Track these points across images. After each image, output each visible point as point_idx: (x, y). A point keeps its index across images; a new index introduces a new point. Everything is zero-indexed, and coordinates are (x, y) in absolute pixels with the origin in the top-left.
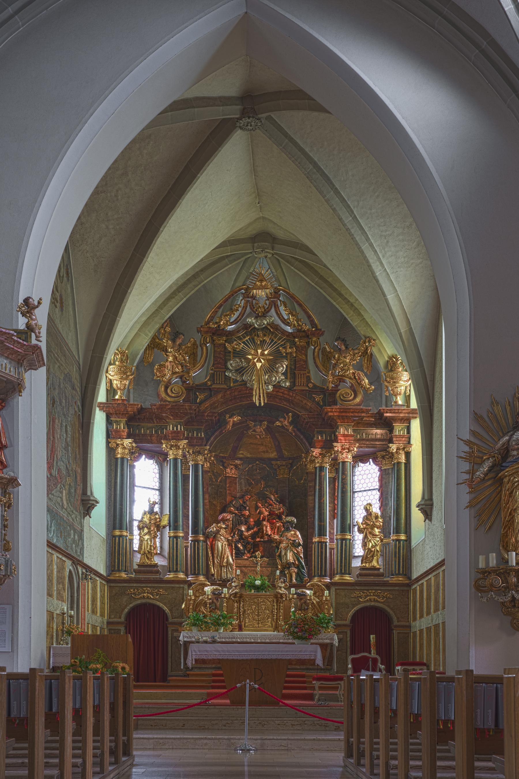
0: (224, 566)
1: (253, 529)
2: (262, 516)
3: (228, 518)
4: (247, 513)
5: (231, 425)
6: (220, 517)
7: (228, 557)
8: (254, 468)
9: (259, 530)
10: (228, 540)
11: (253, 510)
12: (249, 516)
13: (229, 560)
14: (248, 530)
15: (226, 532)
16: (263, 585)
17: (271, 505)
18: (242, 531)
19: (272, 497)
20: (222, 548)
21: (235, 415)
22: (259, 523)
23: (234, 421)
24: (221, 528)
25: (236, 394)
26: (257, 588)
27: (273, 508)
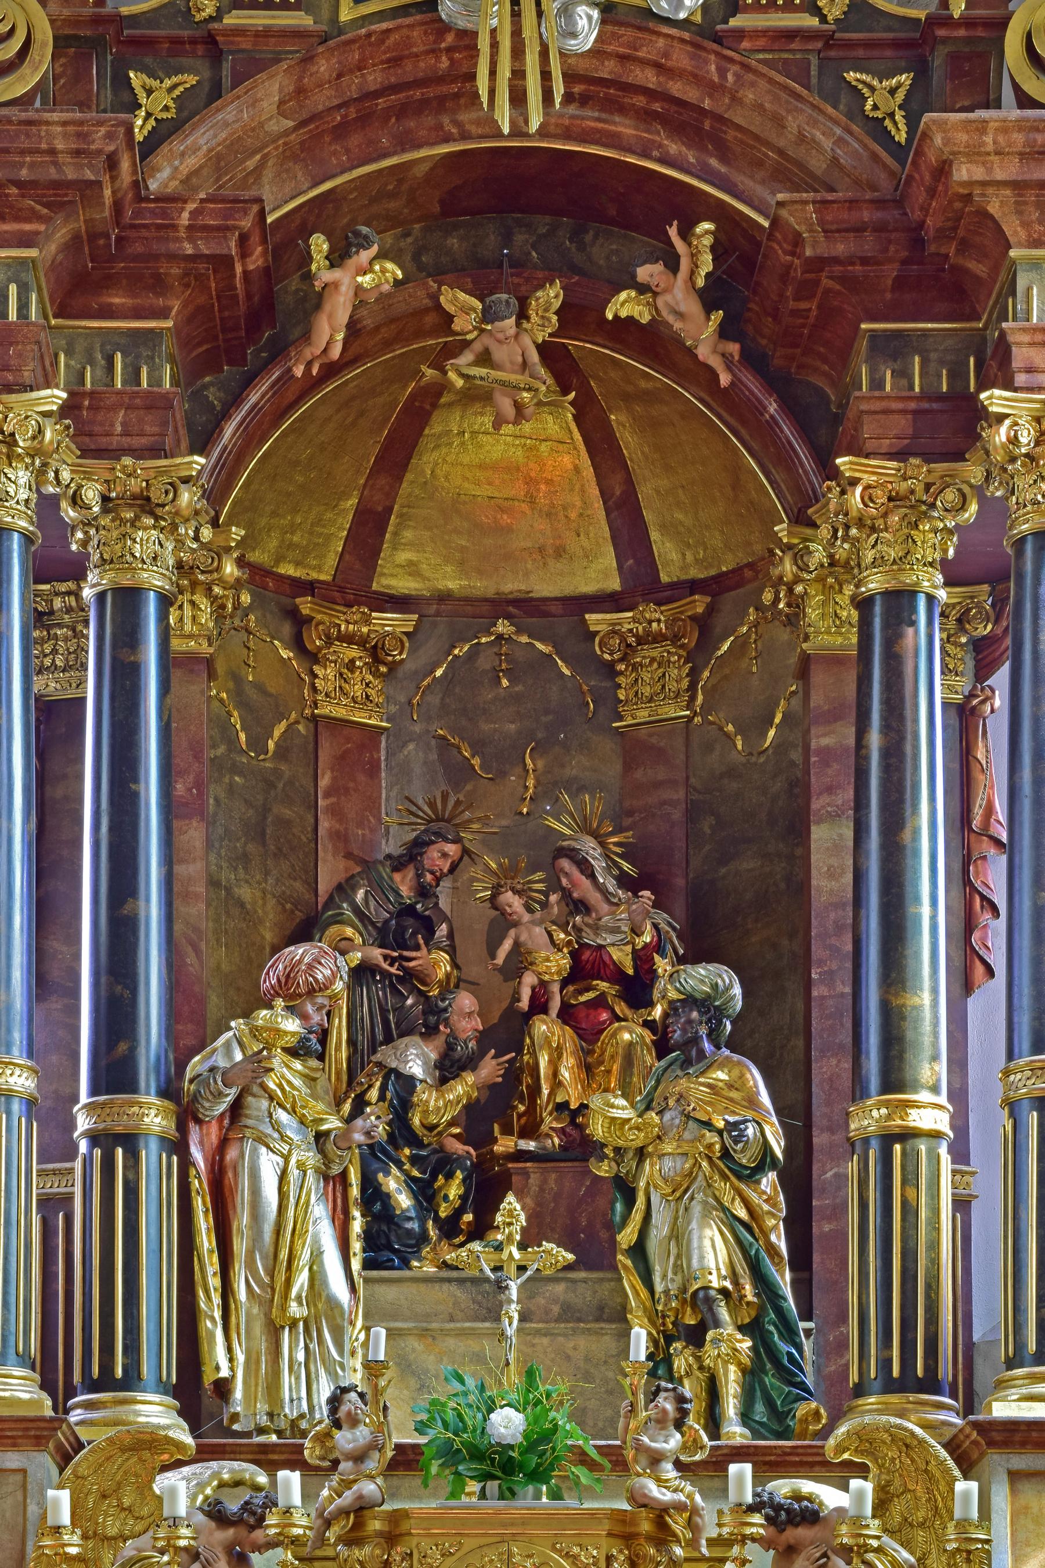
0: (293, 1324)
1: (471, 1063)
2: (529, 980)
3: (322, 974)
4: (441, 965)
5: (343, 317)
6: (269, 980)
7: (317, 1256)
8: (485, 662)
9: (512, 1074)
10: (320, 1137)
11: (472, 949)
12: (448, 987)
13: (325, 1283)
14: (447, 1069)
15: (310, 1080)
16: (539, 1439)
17: (581, 906)
18: (411, 1080)
19: (589, 847)
20: (282, 1195)
21: (365, 243)
22: (509, 1032)
23: (359, 289)
24: (270, 1036)
25: (374, 78)
26: (503, 1467)
27: (596, 929)
